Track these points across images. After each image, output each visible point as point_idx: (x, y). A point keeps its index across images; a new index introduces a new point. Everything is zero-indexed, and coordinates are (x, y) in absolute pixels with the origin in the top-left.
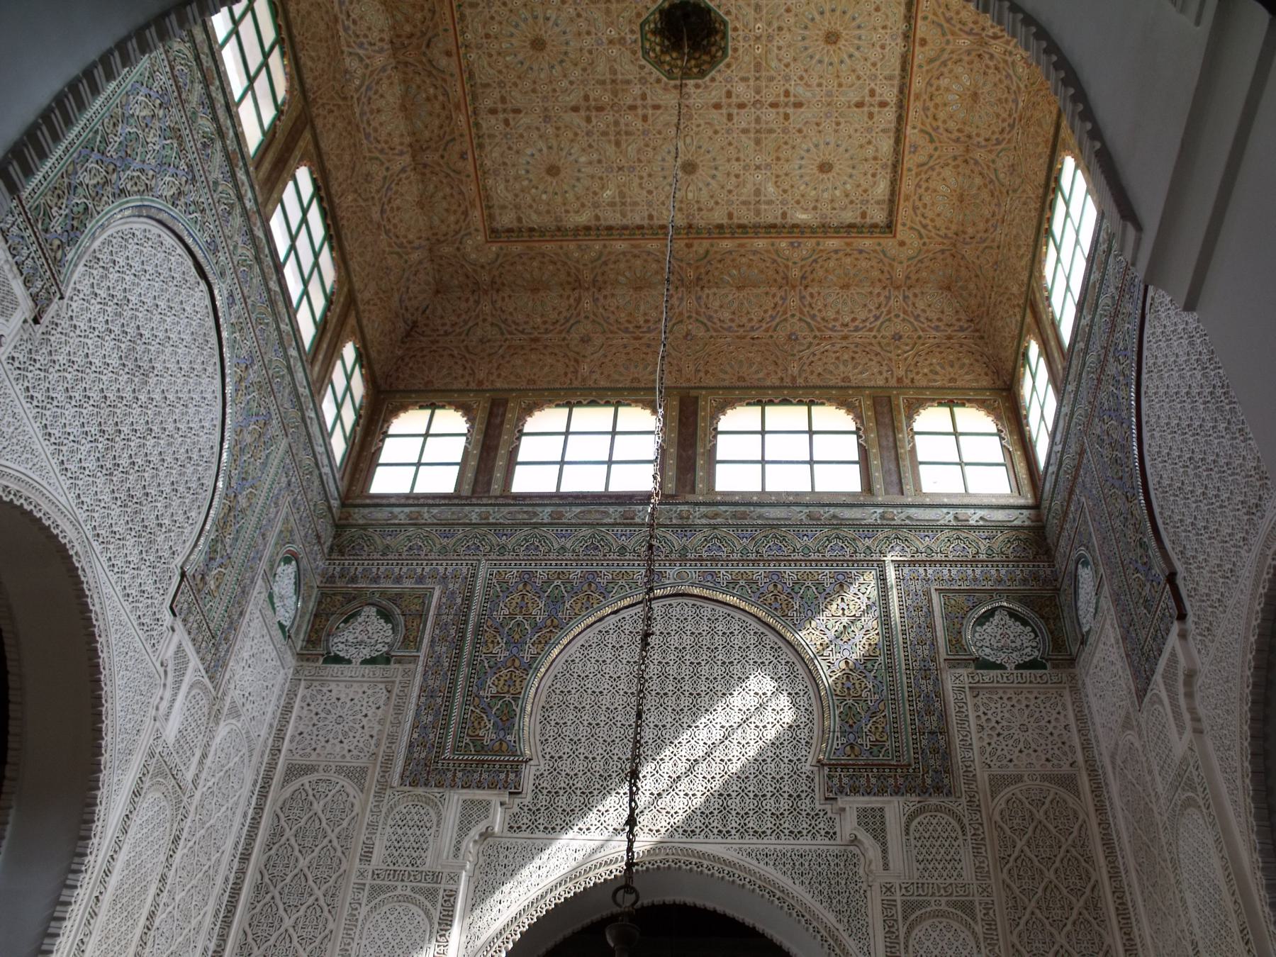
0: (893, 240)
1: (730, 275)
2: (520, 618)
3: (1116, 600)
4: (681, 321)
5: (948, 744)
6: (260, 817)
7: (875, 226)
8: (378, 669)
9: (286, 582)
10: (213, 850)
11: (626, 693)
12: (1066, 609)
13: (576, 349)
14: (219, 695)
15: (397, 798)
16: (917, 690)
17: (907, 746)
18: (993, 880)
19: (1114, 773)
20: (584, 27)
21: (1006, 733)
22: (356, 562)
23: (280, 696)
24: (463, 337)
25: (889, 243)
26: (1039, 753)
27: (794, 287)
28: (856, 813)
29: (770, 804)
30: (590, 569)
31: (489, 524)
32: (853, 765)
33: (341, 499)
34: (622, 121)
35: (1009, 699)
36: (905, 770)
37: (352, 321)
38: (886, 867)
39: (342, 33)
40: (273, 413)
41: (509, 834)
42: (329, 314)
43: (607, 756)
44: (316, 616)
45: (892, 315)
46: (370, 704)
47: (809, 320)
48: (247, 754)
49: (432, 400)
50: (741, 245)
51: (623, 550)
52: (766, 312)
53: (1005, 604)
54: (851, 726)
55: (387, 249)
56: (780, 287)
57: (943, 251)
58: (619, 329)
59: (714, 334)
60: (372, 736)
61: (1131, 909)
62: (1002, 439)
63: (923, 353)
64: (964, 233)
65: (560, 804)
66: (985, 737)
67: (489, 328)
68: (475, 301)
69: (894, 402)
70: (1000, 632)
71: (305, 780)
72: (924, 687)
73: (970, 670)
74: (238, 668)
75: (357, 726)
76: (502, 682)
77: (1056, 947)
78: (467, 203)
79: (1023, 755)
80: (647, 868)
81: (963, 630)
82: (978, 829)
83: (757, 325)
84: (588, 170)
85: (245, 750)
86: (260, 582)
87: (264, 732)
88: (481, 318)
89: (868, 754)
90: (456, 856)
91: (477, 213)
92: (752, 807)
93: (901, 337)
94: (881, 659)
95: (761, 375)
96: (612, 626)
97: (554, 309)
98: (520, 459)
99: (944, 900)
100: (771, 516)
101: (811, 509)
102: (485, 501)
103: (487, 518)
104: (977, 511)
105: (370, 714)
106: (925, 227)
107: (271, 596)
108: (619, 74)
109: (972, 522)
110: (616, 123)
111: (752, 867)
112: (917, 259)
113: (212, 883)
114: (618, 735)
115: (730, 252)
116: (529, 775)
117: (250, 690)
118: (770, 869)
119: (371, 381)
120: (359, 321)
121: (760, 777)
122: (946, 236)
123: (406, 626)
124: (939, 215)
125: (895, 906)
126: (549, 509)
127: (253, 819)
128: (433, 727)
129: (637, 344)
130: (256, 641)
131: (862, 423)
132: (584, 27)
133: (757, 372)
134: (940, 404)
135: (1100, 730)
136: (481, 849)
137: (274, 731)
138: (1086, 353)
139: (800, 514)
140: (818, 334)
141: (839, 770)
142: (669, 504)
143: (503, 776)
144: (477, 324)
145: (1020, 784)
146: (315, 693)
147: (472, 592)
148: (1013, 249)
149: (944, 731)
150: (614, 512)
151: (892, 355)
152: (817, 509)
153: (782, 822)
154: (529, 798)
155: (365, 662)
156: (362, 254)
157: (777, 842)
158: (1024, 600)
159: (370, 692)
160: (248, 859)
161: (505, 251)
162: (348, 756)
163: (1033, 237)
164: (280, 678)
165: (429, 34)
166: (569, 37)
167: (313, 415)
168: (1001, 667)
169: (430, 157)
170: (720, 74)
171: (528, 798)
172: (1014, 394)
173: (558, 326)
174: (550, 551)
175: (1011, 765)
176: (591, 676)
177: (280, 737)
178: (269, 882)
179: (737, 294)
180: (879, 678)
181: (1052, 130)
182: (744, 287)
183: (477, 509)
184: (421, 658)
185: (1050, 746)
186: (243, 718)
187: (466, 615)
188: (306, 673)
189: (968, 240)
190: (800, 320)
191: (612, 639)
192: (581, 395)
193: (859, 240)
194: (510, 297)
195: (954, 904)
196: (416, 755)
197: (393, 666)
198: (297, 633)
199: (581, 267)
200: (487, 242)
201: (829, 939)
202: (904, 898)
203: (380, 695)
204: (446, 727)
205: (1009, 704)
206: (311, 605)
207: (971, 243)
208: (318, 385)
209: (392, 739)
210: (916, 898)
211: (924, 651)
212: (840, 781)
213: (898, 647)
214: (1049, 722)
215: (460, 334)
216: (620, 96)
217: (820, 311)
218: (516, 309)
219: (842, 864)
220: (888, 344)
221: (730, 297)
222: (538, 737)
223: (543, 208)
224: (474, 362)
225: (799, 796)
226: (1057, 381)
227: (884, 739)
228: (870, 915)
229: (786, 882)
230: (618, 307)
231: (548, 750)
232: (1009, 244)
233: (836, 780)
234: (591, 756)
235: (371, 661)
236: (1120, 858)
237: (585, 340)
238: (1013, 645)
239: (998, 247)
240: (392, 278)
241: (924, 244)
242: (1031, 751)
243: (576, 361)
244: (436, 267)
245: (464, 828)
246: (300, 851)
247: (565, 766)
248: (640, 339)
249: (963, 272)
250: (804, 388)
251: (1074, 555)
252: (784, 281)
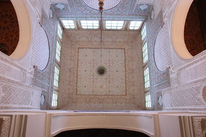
25: (126, 49)
170: (105, 67)
181: (106, 31)
237: (139, 83)
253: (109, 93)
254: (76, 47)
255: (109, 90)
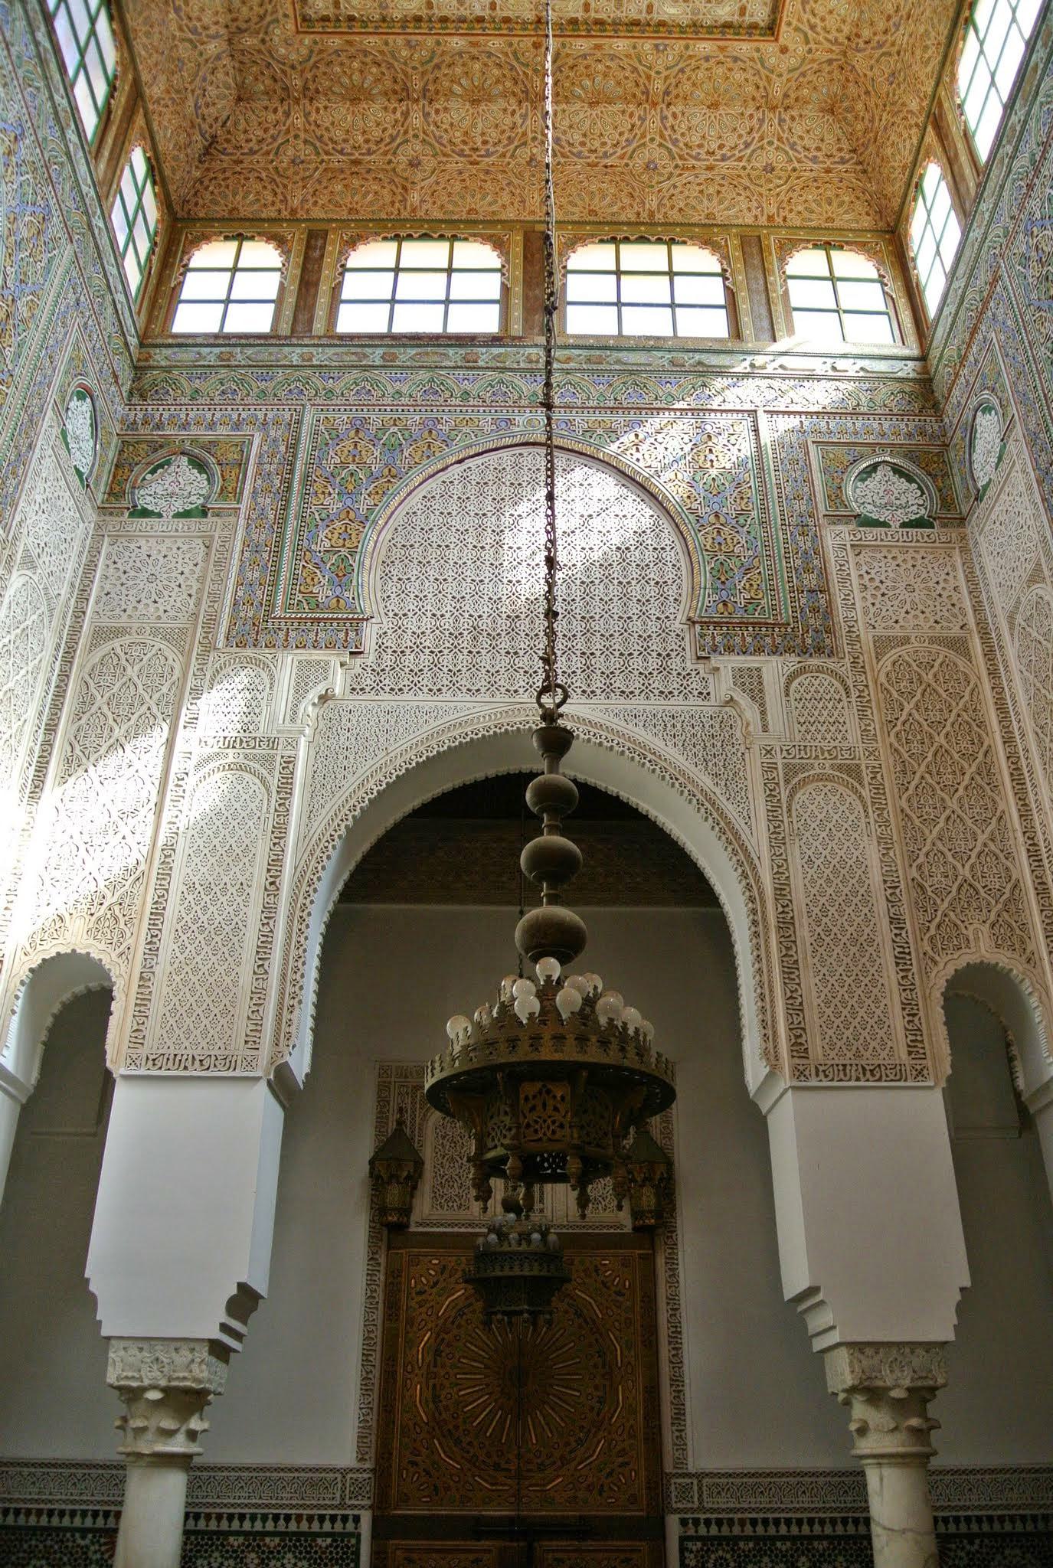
0: (773, 44)
1: (583, 88)
2: (353, 467)
3: (1032, 439)
4: (525, 144)
5: (829, 602)
6: (66, 685)
7: (754, 26)
8: (193, 523)
9: (81, 421)
10: (14, 718)
11: (475, 547)
12: (956, 467)
13: (405, 175)
14: (10, 538)
15: (222, 660)
16: (794, 546)
17: (785, 604)
18: (880, 745)
19: (1012, 634)
21: (891, 593)
22: (161, 408)
23: (81, 553)
24: (271, 157)
25: (770, 48)
26: (927, 615)
27: (655, 104)
28: (731, 673)
29: (637, 663)
30: (429, 415)
31: (313, 366)
32: (727, 623)
33: (138, 337)
35: (894, 558)
36: (783, 629)
37: (140, 121)
38: (765, 728)
40: (53, 209)
41: (352, 697)
42: (112, 101)
43: (457, 613)
44: (117, 465)
45: (765, 141)
46: (186, 560)
47: (671, 146)
48: (47, 613)
49: (239, 228)
50: (598, 47)
51: (466, 394)
52: (621, 134)
53: (888, 459)
54: (723, 583)
55: (178, 34)
56: (640, 104)
57: (830, 62)
58: (453, 151)
59: (562, 160)
60: (190, 595)
61: (1027, 775)
62: (884, 284)
63: (797, 188)
64: (858, 36)
65: (406, 664)
66: (868, 597)
67: (301, 146)
68: (284, 112)
69: (765, 242)
70: (883, 488)
71: (116, 643)
72: (801, 544)
73: (851, 527)
74: (31, 510)
75: (173, 585)
76: (336, 535)
77: (948, 812)
79: (909, 616)
80: (506, 730)
81: (843, 485)
82: (863, 691)
83: (611, 151)
85: (44, 609)
86: (50, 413)
87: (64, 591)
88: (292, 134)
89: (742, 611)
90: (293, 720)
92: (618, 666)
93: (773, 169)
94: (754, 514)
95: (615, 209)
96: (456, 477)
97: (378, 125)
98: (344, 297)
99: (828, 763)
100: (630, 361)
101: (675, 354)
102: (306, 341)
103: (310, 360)
104: (857, 361)
105: (186, 571)
106: (813, 27)
107: (64, 433)
109: (852, 373)
111: (620, 729)
112: (799, 71)
113: (14, 753)
114: (468, 591)
115: (584, 57)
116: (370, 635)
117: (46, 539)
118: (640, 730)
119: (166, 201)
120: (148, 123)
121: (626, 634)
122: (836, 42)
123: (223, 476)
124: (831, 12)
125: (776, 769)
126: (380, 351)
127: (57, 687)
128: (260, 584)
129: (473, 169)
130: (49, 484)
131: (729, 264)
133: (610, 205)
134: (816, 246)
135: (995, 591)
136: (320, 715)
137: (76, 591)
138: (1013, 158)
139: (661, 359)
140: (680, 163)
141: (711, 628)
142: (515, 346)
143: (342, 635)
144: (288, 140)
145: (907, 646)
146: (121, 549)
147: (297, 439)
148: (918, 52)
149: (824, 590)
150: (454, 354)
151: (762, 190)
152: (680, 355)
153: (651, 682)
154: (372, 658)
155: (178, 515)
156: (148, 34)
157: (646, 702)
158: (910, 455)
159: (185, 548)
160: (54, 730)
161: (319, 46)
162: (164, 617)
163: (946, 32)
164: (80, 531)
167: (101, 224)
168: (884, 524)
171: (371, 659)
172: (899, 236)
173: (382, 145)
174: (384, 395)
175: (897, 626)
176: (435, 529)
177: (83, 596)
178: (81, 754)
179: (594, 113)
180: (753, 533)
182: (598, 103)
183: (298, 350)
184: (243, 510)
185: (938, 608)
186: (39, 571)
187: (292, 464)
188: (110, 527)
189: (862, 45)
190: (660, 145)
191: (457, 490)
192: (411, 228)
193: (736, 43)
194: (326, 108)
195: (840, 768)
196: (242, 614)
197: (210, 519)
198: (97, 485)
199: (410, 70)
200: (298, 32)
201: (706, 803)
202: (785, 761)
203: (197, 551)
204: (274, 584)
205: (895, 563)
206: (111, 455)
207: (864, 50)
208: (105, 189)
209: (215, 597)
210: (798, 761)
211: (801, 507)
212: (714, 638)
213: (773, 502)
214: (937, 583)
215: (268, 153)
217: (683, 134)
218: (333, 123)
219: (718, 726)
220: (759, 177)
221: (582, 115)
222: (379, 594)
224: (285, 186)
225: (668, 655)
226: (965, 207)
227: (760, 596)
228: (749, 778)
229: (657, 744)
230: (452, 125)
231: (392, 607)
232: (914, 45)
233: (708, 639)
234: (438, 614)
235: (186, 514)
236: (1015, 723)
237: (414, 164)
238: (898, 502)
239: (898, 53)
240: (185, 74)
241: (810, 51)
242: (918, 612)
243: (405, 188)
244: (237, 65)
245: (300, 689)
246: (115, 721)
247: (411, 624)
248: (477, 164)
249: (852, 89)
250: (662, 224)
251: (974, 402)
252: (644, 98)
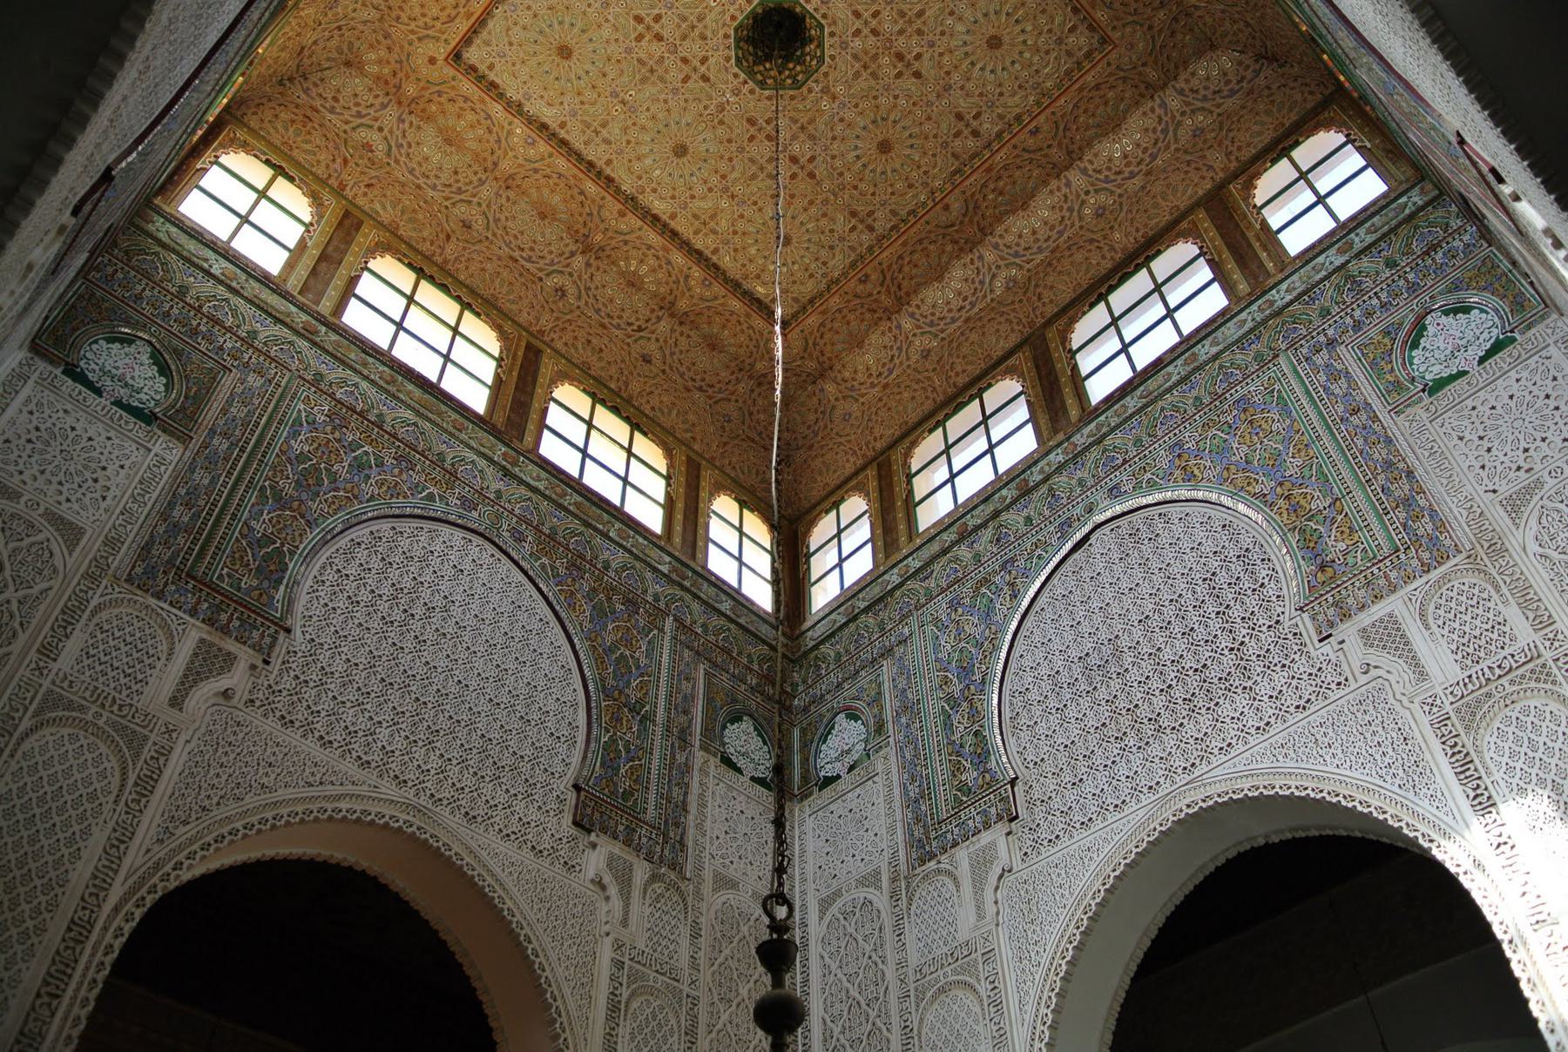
20: (839, 127)
34: (897, 28)
39: (976, 310)
78: (1085, 93)
84: (968, 14)
91: (1089, 78)
108: (855, 69)
110: (901, 32)
132: (839, 127)
161: (1115, 23)
165: (942, 231)
166: (858, 131)
169: (1057, 154)
216: (874, 51)
223: (1042, 20)
253: (975, 133)
254: (434, 73)
255: (959, 117)
